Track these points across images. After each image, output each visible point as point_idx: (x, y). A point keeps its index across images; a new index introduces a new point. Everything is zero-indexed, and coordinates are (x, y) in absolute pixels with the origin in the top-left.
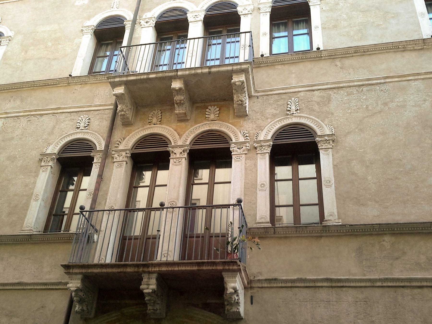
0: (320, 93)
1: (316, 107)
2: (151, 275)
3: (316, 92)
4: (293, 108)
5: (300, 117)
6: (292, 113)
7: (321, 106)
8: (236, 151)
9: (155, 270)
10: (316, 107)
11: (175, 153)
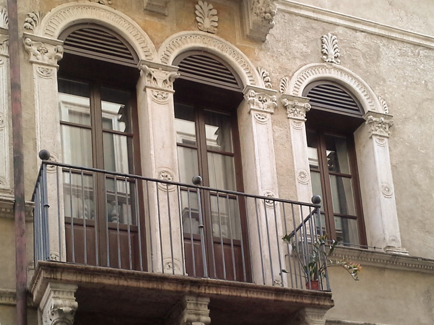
0: (365, 38)
1: (362, 62)
2: (199, 299)
3: (358, 34)
4: (332, 52)
5: (341, 70)
6: (330, 60)
7: (367, 62)
8: (258, 105)
9: (211, 292)
10: (362, 62)
11: (154, 79)
